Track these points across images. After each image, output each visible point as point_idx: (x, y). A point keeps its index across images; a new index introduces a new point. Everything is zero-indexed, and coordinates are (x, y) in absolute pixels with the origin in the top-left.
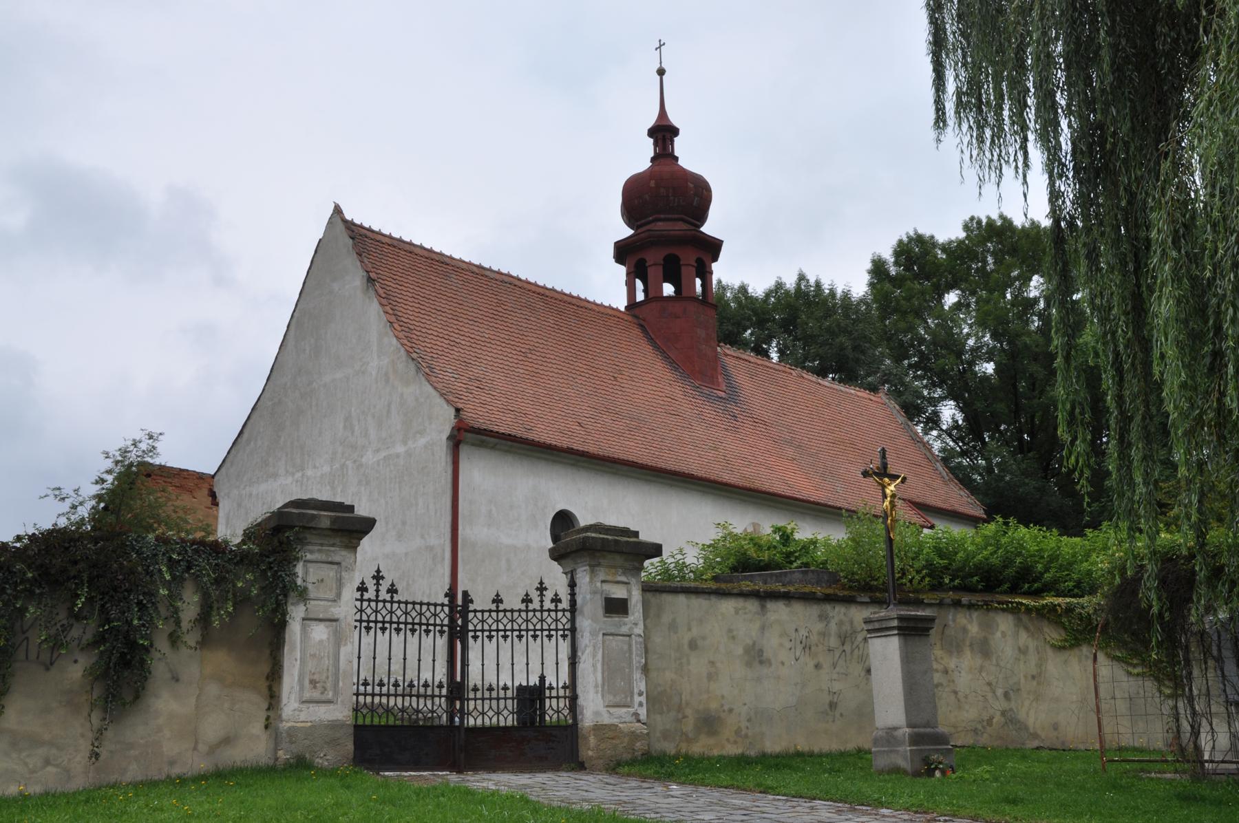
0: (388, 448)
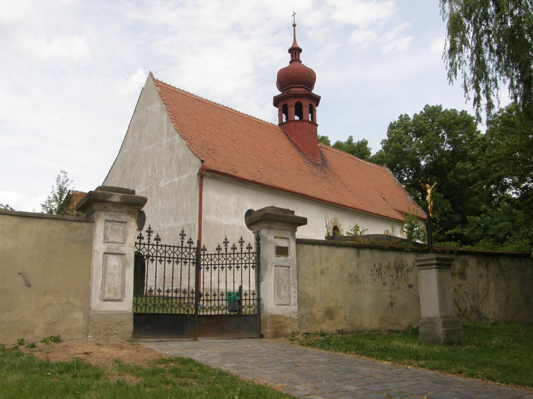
0: (171, 179)
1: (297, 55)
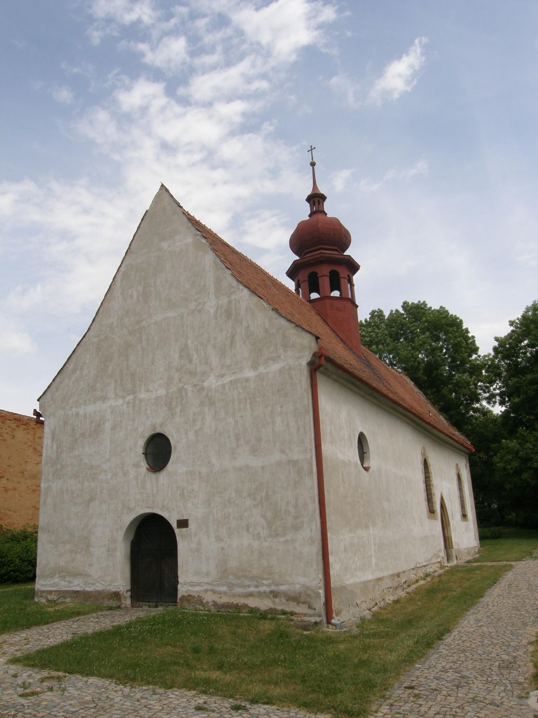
1: (321, 204)
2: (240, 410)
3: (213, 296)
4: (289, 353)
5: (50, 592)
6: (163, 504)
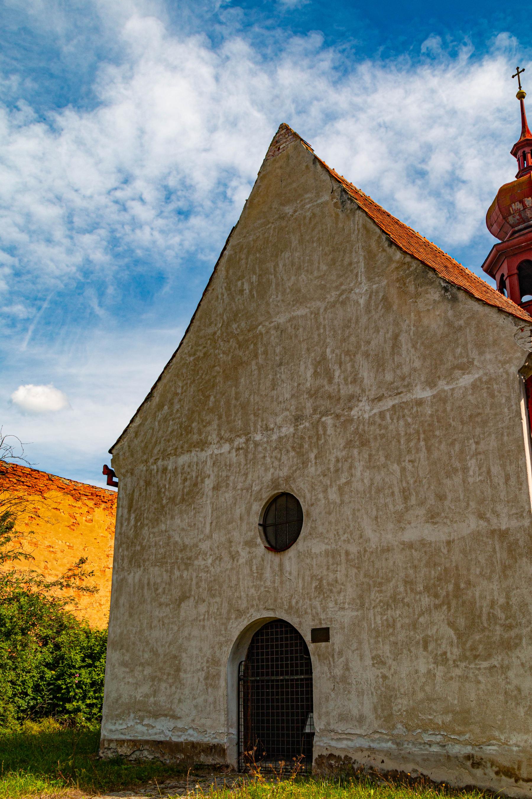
2: (409, 452)
3: (363, 278)
4: (488, 356)
5: (121, 742)
6: (290, 602)
